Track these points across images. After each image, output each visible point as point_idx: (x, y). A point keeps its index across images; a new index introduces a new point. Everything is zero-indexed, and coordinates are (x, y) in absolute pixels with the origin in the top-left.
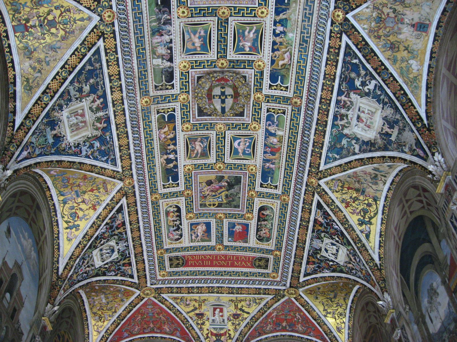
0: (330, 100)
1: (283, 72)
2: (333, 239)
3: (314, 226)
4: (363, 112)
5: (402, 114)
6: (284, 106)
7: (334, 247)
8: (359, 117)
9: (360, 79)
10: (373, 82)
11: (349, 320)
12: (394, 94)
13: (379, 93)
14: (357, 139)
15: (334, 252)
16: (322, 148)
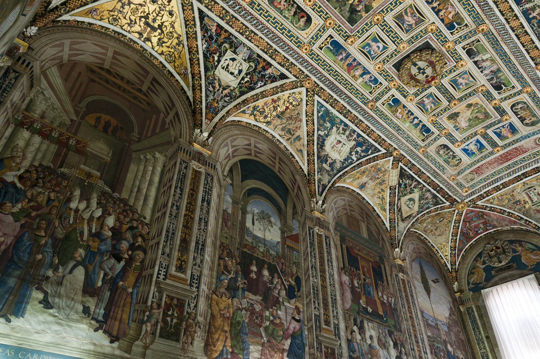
0: (358, 127)
1: (394, 108)
2: (247, 74)
3: (265, 60)
4: (342, 147)
5: (336, 174)
6: (375, 95)
7: (236, 72)
8: (340, 142)
9: (360, 152)
10: (355, 159)
11: (103, 27)
12: (346, 172)
13: (349, 161)
14: (327, 136)
15: (231, 69)
16: (331, 105)
